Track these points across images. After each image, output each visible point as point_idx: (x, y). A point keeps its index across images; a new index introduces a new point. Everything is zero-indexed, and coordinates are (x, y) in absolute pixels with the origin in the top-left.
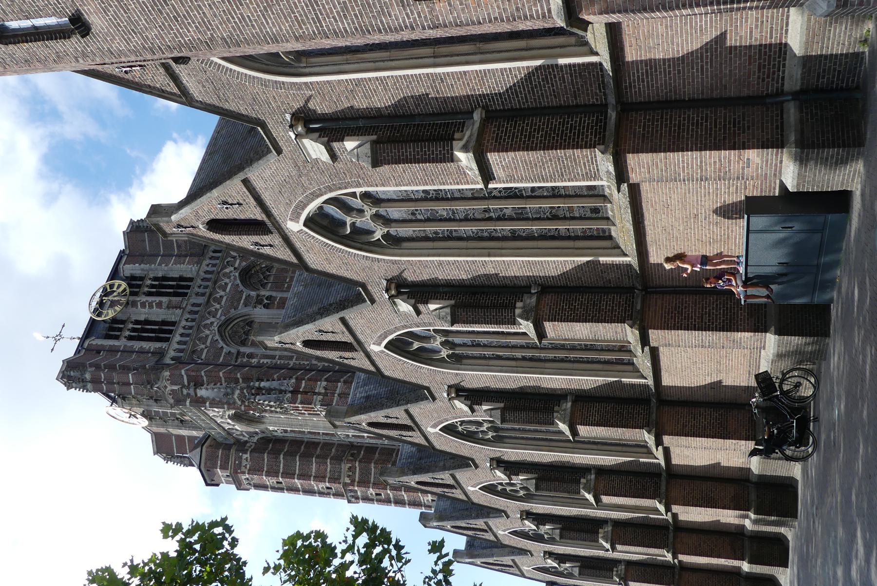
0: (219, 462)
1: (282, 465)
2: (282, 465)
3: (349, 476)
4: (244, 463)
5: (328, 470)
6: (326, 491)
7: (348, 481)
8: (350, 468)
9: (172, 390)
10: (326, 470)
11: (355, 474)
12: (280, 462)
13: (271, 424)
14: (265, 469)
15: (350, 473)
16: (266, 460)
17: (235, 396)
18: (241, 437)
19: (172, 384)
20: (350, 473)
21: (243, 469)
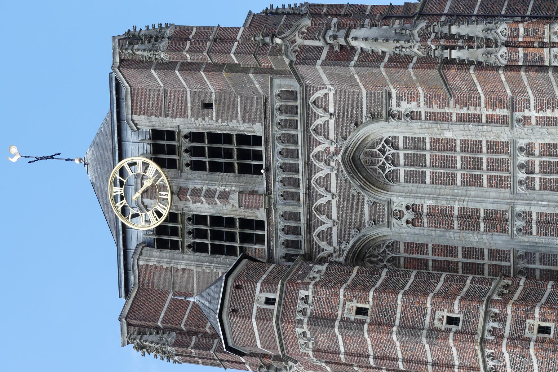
0: (264, 276)
1: (380, 282)
2: (380, 282)
3: (501, 294)
4: (312, 274)
5: (465, 289)
6: (444, 326)
7: (496, 297)
8: (507, 287)
9: (302, 47)
10: (461, 290)
11: (513, 293)
12: (379, 278)
13: (401, 193)
14: (348, 283)
15: (506, 291)
16: (353, 276)
17: (415, 32)
18: (323, 244)
19: (305, 38)
20: (506, 291)
21: (307, 280)
